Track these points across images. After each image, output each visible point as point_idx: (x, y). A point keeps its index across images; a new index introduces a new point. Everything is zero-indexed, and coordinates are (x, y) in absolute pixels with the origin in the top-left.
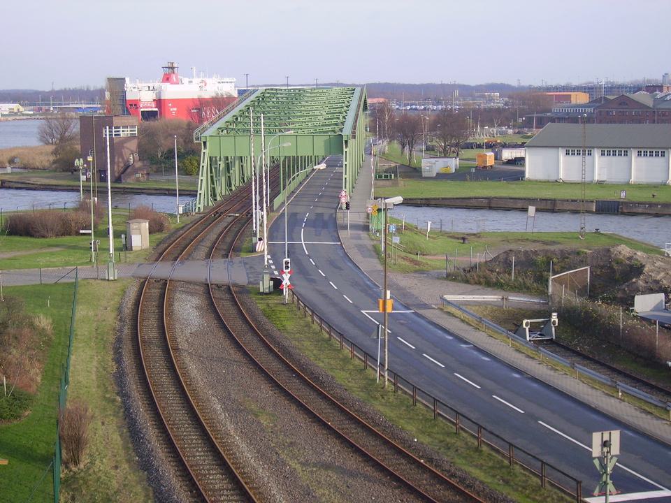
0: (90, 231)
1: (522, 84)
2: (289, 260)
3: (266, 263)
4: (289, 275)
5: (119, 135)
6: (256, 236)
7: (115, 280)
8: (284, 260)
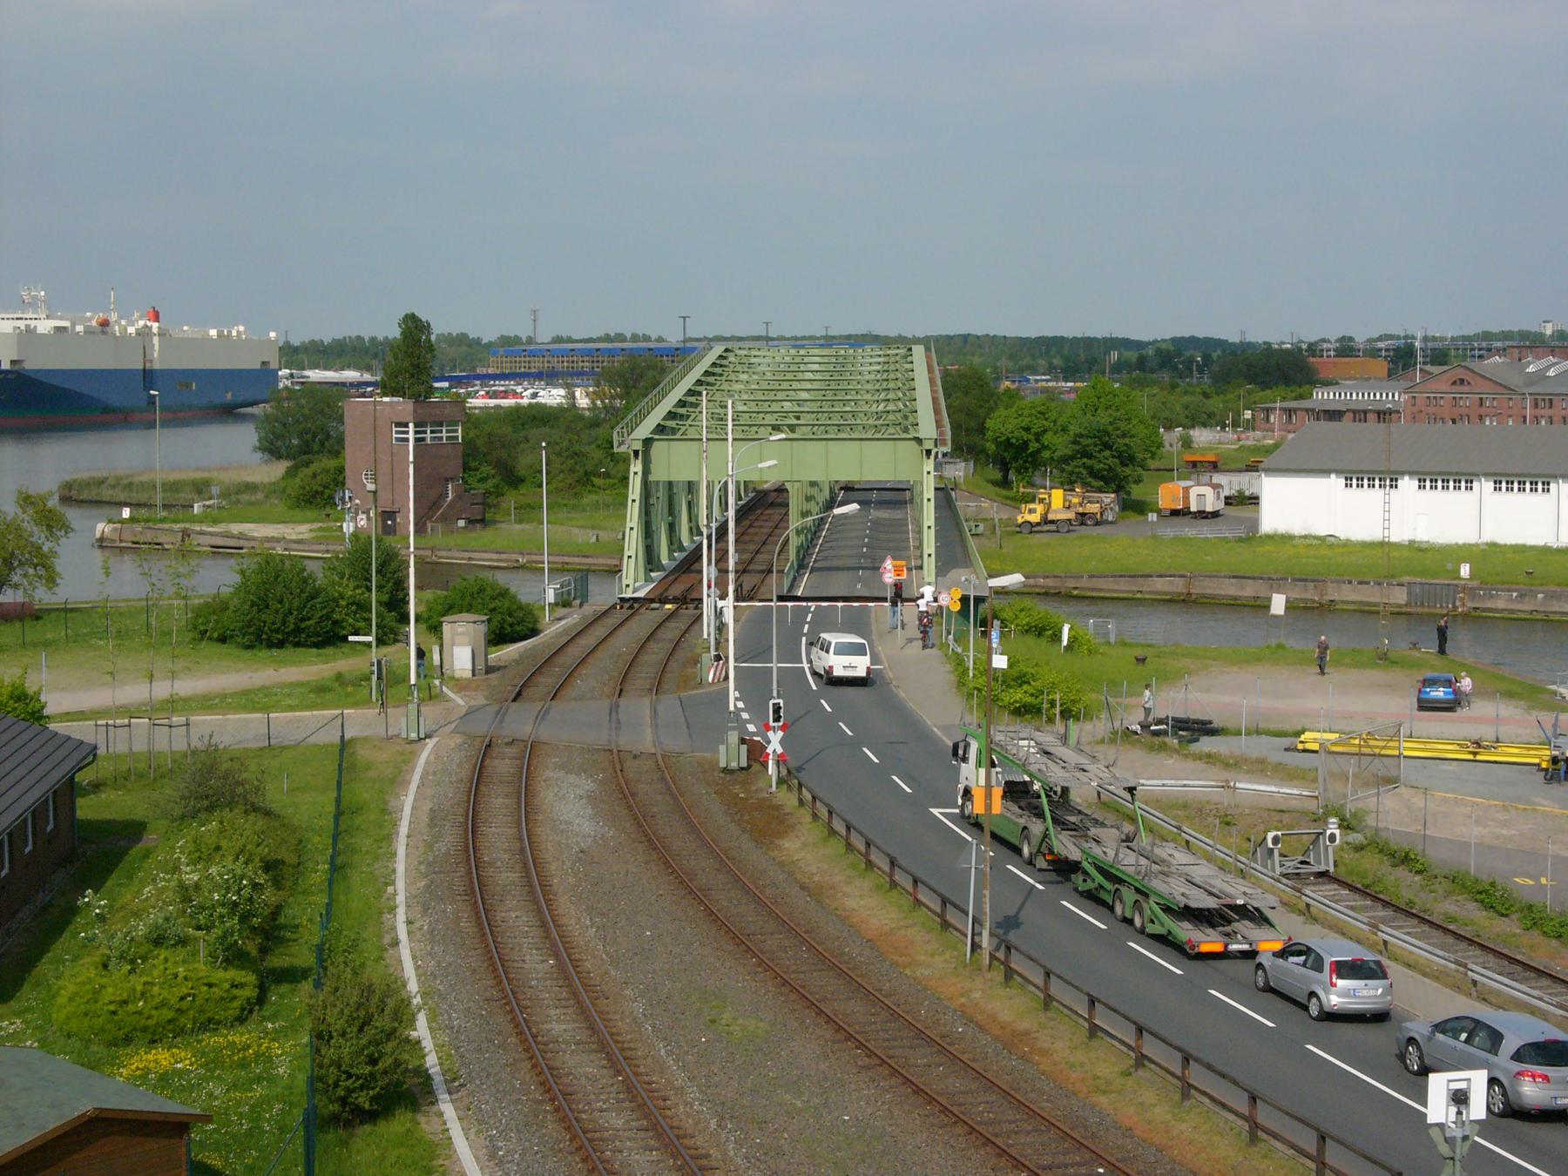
1: (1250, 338)
3: (732, 708)
4: (780, 734)
5: (423, 439)
6: (709, 652)
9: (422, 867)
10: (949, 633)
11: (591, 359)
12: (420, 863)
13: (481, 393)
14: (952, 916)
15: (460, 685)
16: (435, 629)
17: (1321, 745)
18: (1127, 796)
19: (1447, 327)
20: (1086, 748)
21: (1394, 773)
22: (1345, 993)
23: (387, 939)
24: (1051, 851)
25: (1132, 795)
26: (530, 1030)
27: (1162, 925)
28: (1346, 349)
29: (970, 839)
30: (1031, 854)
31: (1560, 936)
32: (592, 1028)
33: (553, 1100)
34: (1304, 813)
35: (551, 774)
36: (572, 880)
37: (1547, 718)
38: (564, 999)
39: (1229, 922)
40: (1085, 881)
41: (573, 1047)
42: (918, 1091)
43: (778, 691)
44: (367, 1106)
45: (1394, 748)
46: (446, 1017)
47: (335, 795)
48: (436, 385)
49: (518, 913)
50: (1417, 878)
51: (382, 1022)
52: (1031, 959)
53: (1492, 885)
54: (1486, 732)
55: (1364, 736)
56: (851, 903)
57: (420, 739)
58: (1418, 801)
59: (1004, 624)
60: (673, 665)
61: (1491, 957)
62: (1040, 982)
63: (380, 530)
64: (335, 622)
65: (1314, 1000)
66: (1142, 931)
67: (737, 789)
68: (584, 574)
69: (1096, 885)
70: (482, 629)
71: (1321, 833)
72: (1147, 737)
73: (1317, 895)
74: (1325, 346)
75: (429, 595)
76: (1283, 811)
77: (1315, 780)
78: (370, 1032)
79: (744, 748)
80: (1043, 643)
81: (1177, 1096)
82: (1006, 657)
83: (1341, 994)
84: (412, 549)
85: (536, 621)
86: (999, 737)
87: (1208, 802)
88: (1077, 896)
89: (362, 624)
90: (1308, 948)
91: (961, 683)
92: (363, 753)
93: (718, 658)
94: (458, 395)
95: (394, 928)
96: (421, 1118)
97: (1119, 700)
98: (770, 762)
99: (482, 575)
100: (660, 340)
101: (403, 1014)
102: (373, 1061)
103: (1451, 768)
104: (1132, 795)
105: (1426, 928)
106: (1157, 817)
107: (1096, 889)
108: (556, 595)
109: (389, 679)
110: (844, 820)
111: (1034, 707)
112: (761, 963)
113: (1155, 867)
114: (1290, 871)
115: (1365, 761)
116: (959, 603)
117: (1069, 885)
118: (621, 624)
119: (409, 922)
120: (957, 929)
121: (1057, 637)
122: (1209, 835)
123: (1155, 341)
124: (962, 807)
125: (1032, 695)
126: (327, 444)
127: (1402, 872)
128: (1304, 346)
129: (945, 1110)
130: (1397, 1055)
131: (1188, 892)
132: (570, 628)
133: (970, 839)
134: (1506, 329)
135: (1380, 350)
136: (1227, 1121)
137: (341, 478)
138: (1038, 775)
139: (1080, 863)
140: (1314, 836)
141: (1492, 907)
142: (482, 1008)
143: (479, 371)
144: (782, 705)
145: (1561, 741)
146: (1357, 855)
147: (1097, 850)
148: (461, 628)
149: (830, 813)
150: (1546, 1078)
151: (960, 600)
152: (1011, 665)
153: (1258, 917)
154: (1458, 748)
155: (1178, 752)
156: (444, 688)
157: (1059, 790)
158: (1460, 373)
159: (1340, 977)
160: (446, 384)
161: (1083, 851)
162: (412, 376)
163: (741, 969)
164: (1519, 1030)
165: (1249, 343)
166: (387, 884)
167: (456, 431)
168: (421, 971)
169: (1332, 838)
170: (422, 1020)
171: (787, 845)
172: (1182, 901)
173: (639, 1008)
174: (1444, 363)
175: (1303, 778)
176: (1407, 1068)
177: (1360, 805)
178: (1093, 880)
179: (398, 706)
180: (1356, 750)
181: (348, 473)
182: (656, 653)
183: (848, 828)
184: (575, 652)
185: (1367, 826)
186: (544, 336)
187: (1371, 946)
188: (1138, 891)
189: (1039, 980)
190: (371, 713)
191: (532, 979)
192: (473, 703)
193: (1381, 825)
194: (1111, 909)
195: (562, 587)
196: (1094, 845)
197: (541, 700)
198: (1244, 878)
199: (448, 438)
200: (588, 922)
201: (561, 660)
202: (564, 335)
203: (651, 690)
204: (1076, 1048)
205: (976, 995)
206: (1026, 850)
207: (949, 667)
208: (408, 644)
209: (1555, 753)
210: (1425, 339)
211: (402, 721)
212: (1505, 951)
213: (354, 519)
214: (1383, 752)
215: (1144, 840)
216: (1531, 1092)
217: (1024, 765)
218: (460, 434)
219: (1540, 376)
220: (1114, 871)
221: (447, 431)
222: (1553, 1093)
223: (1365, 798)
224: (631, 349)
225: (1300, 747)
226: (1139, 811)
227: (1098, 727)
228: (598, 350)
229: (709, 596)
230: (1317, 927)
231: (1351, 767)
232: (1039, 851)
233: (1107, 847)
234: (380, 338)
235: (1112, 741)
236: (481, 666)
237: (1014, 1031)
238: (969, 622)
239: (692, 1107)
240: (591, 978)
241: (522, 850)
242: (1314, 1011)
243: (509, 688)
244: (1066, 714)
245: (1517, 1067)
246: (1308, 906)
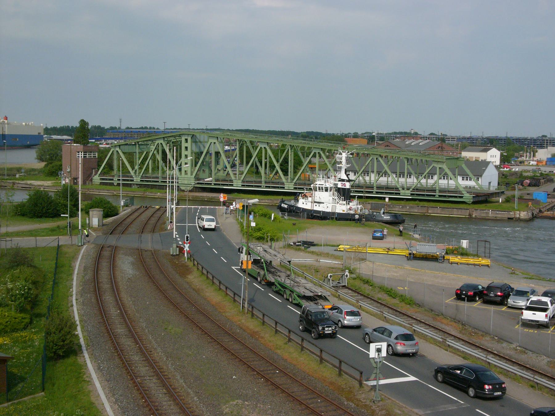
0: (67, 215)
2: (189, 235)
3: (174, 237)
4: (188, 245)
5: (86, 157)
8: (186, 235)
9: (81, 283)
10: (239, 216)
11: (137, 134)
12: (80, 282)
13: (104, 143)
14: (237, 298)
15: (95, 230)
16: (88, 213)
17: (344, 249)
18: (288, 263)
19: (385, 130)
20: (277, 250)
21: (365, 257)
22: (349, 320)
23: (70, 305)
24: (266, 279)
25: (290, 263)
26: (111, 331)
27: (297, 301)
28: (356, 136)
29: (242, 275)
30: (260, 280)
31: (410, 304)
32: (130, 331)
33: (117, 352)
34: (339, 269)
35: (120, 256)
36: (126, 287)
37: (408, 242)
38: (122, 322)
39: (317, 300)
40: (276, 288)
41: (124, 336)
42: (225, 349)
43: (188, 233)
44: (61, 354)
46: (86, 328)
47: (55, 262)
48: (90, 141)
49: (109, 297)
50: (371, 287)
51: (66, 329)
52: (259, 311)
53: (391, 289)
54: (391, 246)
56: (207, 294)
57: (82, 245)
58: (371, 265)
59: (255, 213)
60: (158, 224)
61: (390, 310)
62: (262, 317)
63: (72, 183)
64: (58, 211)
65: (340, 322)
66: (292, 302)
67: (175, 261)
68: (132, 198)
69: (279, 289)
70: (102, 213)
71: (343, 275)
72: (295, 247)
73: (342, 292)
74: (350, 135)
75: (86, 203)
76: (333, 268)
77: (343, 259)
78: (63, 332)
79: (178, 249)
80: (266, 219)
81: (300, 350)
82: (255, 223)
83: (348, 320)
84: (80, 189)
85: (118, 211)
86: (252, 246)
87: (312, 265)
88: (273, 293)
89: (66, 211)
90: (338, 307)
91: (242, 231)
92: (65, 250)
93: (171, 222)
94: (97, 143)
95: (72, 301)
96: (78, 358)
97: (288, 236)
98: (185, 253)
99: (102, 197)
100: (158, 129)
101: (73, 326)
102: (63, 341)
103: (381, 256)
104: (290, 263)
105: (372, 301)
106: (297, 270)
107: (279, 290)
108: (124, 203)
109: (73, 228)
110: (206, 270)
111: (262, 237)
112: (181, 312)
113: (295, 284)
114: (334, 285)
115: (357, 254)
117: (271, 289)
118: (143, 212)
119: (76, 300)
120: (238, 302)
121: (270, 217)
122: (312, 275)
123: (302, 132)
124: (241, 266)
125: (262, 234)
126: (57, 158)
127: (366, 286)
128: (344, 135)
129: (233, 354)
130: (363, 338)
131: (305, 291)
132: (128, 213)
133: (242, 275)
134: (401, 131)
135: (365, 136)
136: (314, 357)
137: (61, 168)
138: (263, 258)
139: (274, 283)
141: (391, 296)
142: (97, 325)
143: (104, 137)
145: (412, 249)
146: (354, 281)
147: (279, 279)
148: (95, 213)
149: (202, 268)
150: (404, 344)
151: (242, 206)
152: (256, 225)
153: (325, 299)
154: (383, 250)
155: (304, 251)
156: (90, 230)
157: (269, 261)
158: (387, 144)
159: (347, 316)
160: (94, 141)
161: (275, 279)
162: (83, 138)
163: (175, 313)
164: (397, 330)
165: (329, 134)
166: (70, 288)
167: (96, 154)
168: (79, 314)
169: (347, 276)
170: (79, 328)
171: (189, 277)
172: (303, 294)
173: (144, 325)
174: (383, 141)
175: (339, 259)
176: (366, 342)
177: (355, 266)
178: (278, 288)
179: (75, 236)
180: (354, 251)
181: (63, 167)
183: (207, 272)
184: (129, 220)
185: (357, 272)
186: (123, 127)
187: (357, 307)
188: (291, 291)
189: (261, 317)
190: (67, 237)
191: (113, 316)
192: (98, 235)
193: (361, 272)
194: (283, 296)
195: (126, 201)
196: (278, 277)
197: (119, 234)
198: (321, 287)
199: (93, 156)
200: (130, 300)
201: (125, 222)
202: (130, 127)
203: (151, 231)
204: (271, 336)
205: (243, 321)
206: (259, 279)
207: (239, 226)
208: (79, 217)
209: (410, 252)
210: (378, 134)
211: (76, 240)
212: (395, 308)
213: (65, 180)
214: (362, 251)
215: (293, 276)
216: (400, 348)
217: (259, 254)
218: (97, 155)
219: (410, 145)
220: (284, 285)
221: (93, 154)
222: (406, 349)
223: (356, 264)
224: (149, 131)
225: (339, 250)
226: (291, 268)
227: (281, 244)
228: (139, 131)
229: (169, 204)
230: (341, 301)
231: (352, 255)
232: (263, 279)
233: (282, 279)
234: (75, 126)
235: (284, 247)
237: (254, 331)
238: (244, 212)
239: (159, 354)
240: (130, 316)
241: (111, 279)
242: (340, 325)
243: (109, 231)
244: (272, 240)
245: (396, 341)
246: (339, 295)
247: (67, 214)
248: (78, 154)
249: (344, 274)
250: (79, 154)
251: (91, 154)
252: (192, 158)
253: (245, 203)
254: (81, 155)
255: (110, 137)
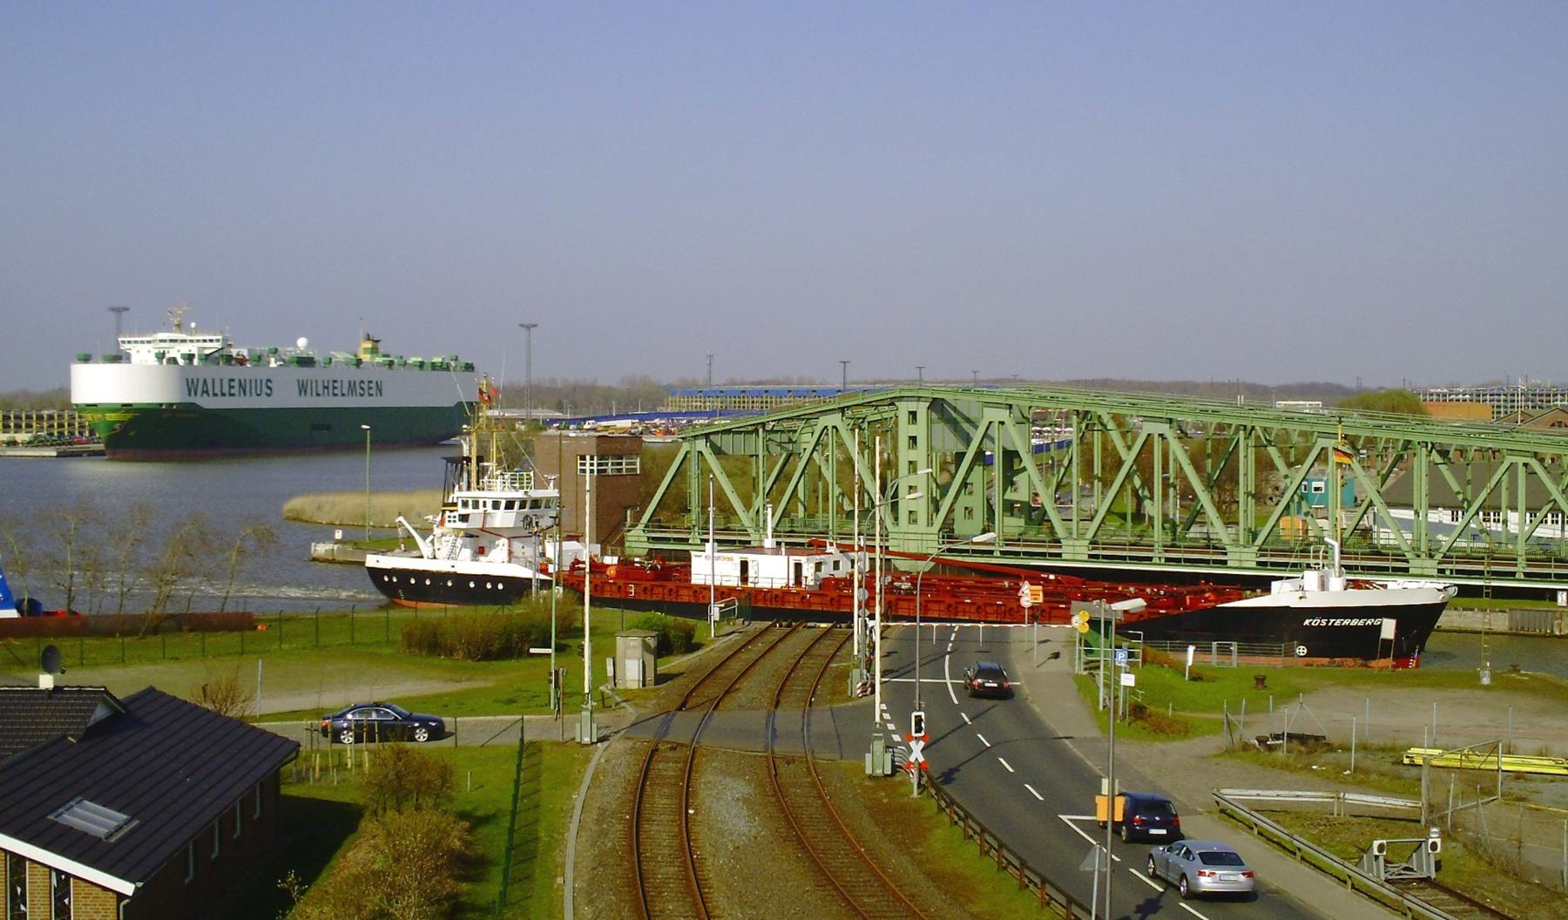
2: (922, 714)
3: (878, 719)
4: (922, 744)
5: (605, 470)
7: (592, 743)
8: (915, 714)
11: (760, 400)
15: (629, 697)
17: (1424, 759)
29: (1094, 843)
35: (711, 778)
45: (1492, 762)
55: (1466, 752)
57: (592, 743)
116: (1086, 624)
118: (781, 640)
133: (1094, 843)
140: (1418, 844)
144: (923, 717)
151: (1088, 622)
154: (1553, 763)
167: (634, 464)
169: (1434, 846)
182: (811, 667)
184: (736, 666)
199: (626, 469)
201: (723, 673)
214: (1482, 767)
236: (650, 677)
247: (550, 647)
248: (581, 464)
249: (1426, 842)
250: (584, 465)
251: (621, 464)
252: (930, 470)
253: (1099, 612)
254: (592, 465)
255: (677, 410)
